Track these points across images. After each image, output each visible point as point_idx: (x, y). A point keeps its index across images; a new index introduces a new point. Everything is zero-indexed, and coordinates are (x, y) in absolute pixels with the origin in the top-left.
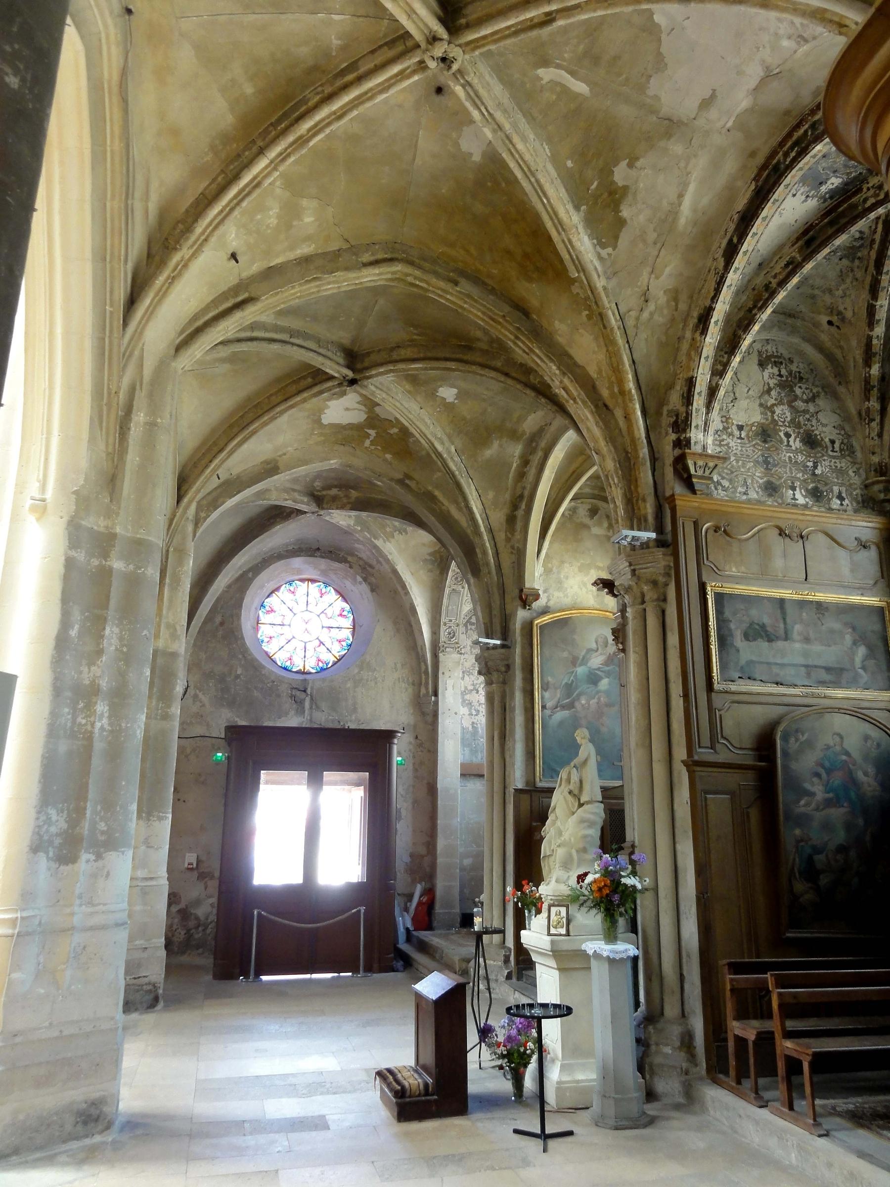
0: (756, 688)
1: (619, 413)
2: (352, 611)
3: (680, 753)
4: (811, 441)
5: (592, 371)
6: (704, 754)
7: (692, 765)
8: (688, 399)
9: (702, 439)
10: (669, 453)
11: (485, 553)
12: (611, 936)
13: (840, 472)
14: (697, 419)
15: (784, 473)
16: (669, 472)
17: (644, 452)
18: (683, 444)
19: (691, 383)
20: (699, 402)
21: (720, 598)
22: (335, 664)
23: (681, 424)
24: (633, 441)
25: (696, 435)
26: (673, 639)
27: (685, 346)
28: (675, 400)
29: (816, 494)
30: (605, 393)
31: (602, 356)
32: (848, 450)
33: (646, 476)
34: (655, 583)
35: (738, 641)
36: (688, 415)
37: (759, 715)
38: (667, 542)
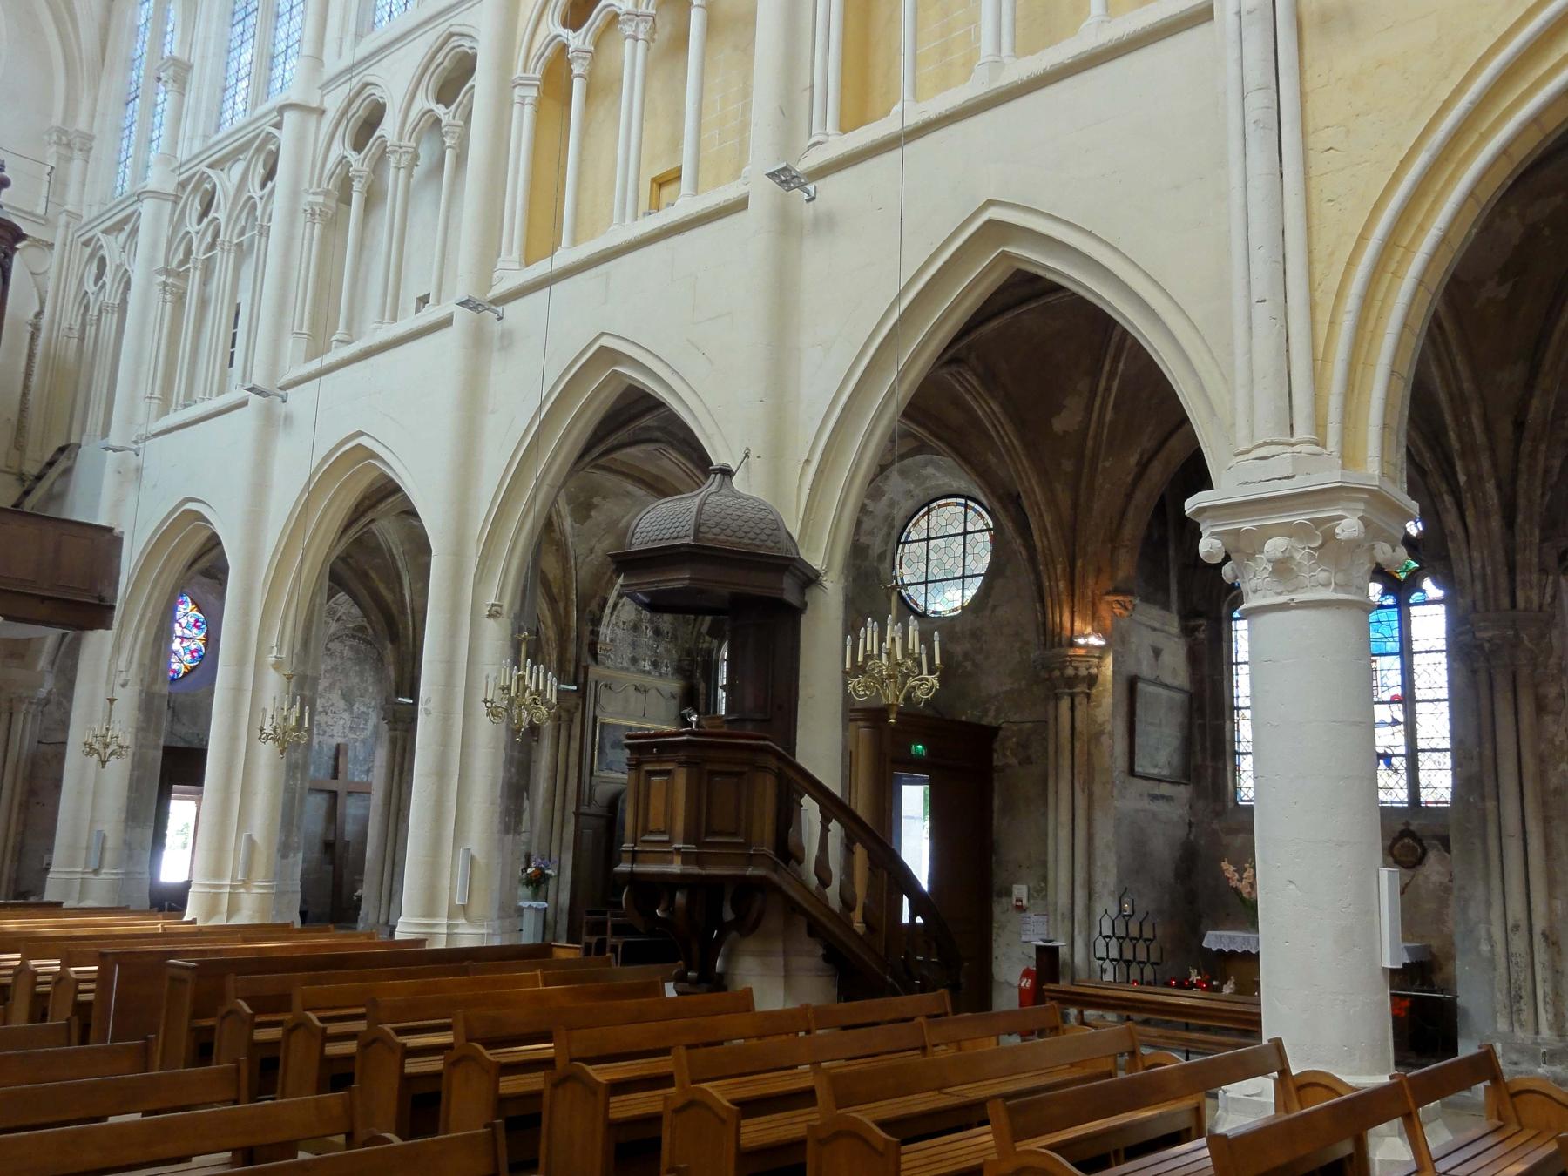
0: (613, 775)
1: (561, 605)
2: (206, 622)
3: (571, 807)
4: (657, 632)
5: (551, 577)
6: (584, 809)
7: (577, 814)
8: (602, 608)
9: (605, 631)
10: (587, 638)
11: (406, 628)
12: (535, 898)
13: (669, 651)
14: (605, 621)
15: (641, 651)
16: (585, 649)
17: (574, 635)
18: (595, 633)
19: (605, 601)
20: (607, 611)
21: (602, 724)
22: (186, 674)
23: (596, 622)
24: (567, 625)
25: (603, 630)
26: (575, 745)
27: (606, 578)
28: (594, 606)
29: (655, 664)
30: (555, 591)
31: (559, 572)
32: (675, 638)
33: (572, 649)
34: (568, 711)
35: (608, 750)
36: (600, 619)
37: (612, 788)
38: (582, 693)
